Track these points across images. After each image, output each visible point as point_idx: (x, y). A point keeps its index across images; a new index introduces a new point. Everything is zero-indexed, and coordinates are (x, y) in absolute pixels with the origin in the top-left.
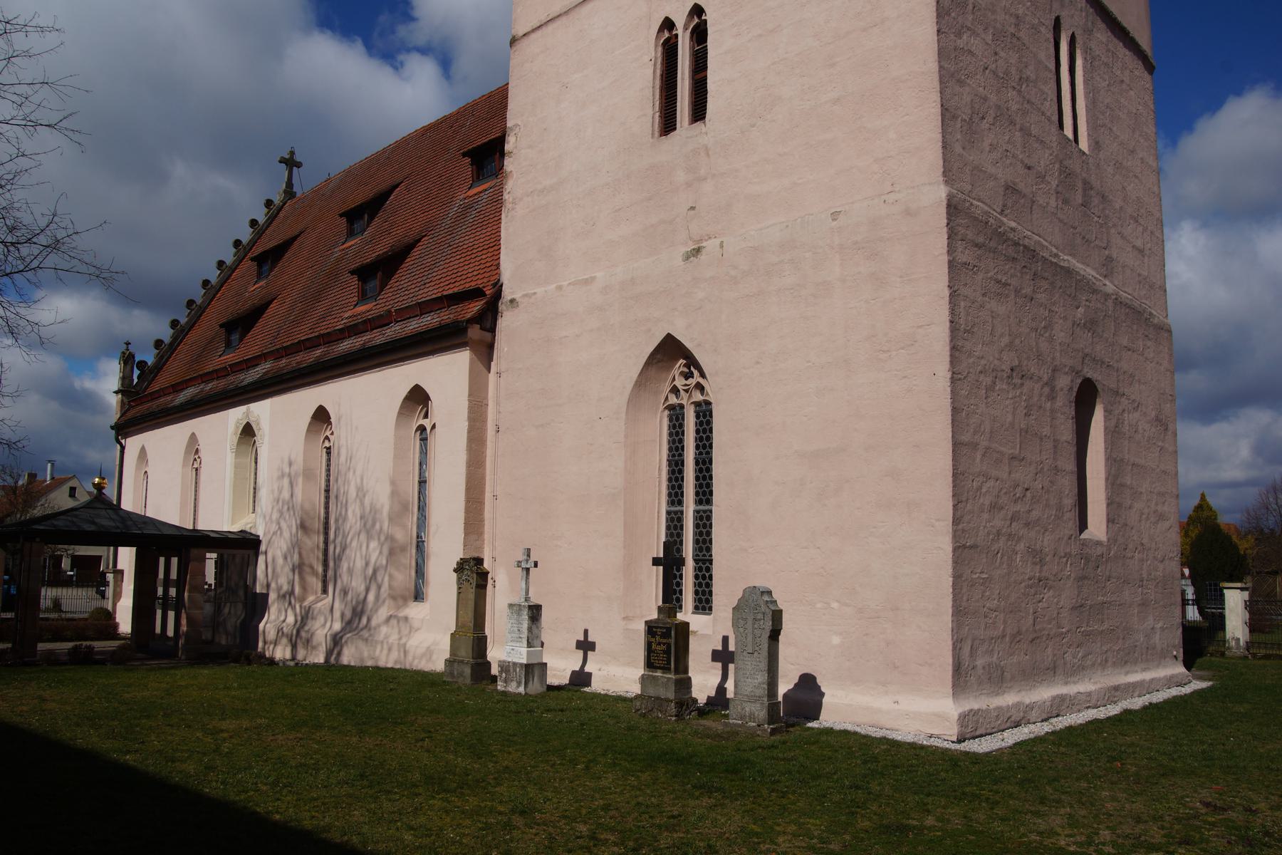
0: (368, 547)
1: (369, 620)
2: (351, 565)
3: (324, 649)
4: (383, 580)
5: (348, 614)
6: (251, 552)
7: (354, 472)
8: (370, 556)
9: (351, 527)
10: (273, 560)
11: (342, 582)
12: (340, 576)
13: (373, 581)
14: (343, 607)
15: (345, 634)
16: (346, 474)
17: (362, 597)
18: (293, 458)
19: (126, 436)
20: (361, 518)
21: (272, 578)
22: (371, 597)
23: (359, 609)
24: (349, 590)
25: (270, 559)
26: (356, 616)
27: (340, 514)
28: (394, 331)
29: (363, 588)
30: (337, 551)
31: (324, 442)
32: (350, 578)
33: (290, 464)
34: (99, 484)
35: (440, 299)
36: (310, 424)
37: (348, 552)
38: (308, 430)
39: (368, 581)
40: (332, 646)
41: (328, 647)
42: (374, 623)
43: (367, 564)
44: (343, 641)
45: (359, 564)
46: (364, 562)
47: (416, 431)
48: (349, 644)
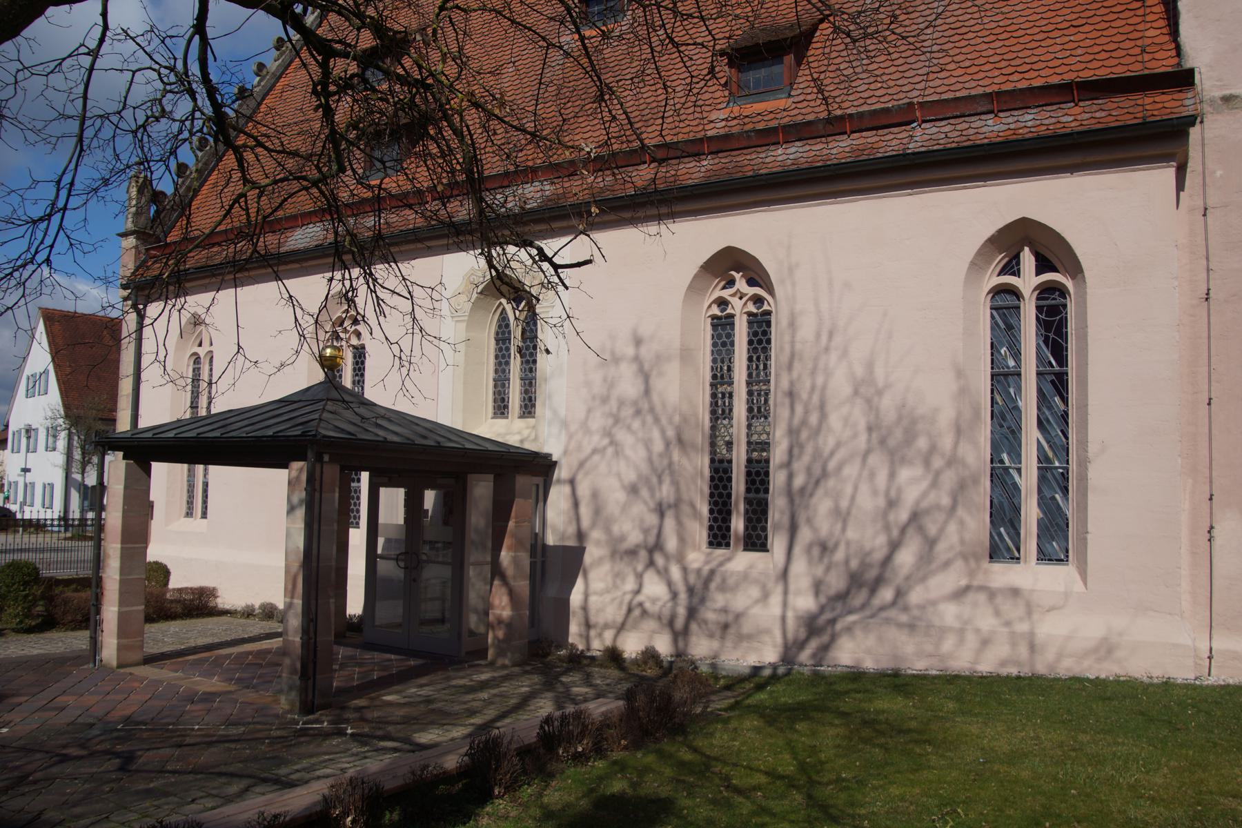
0: (892, 475)
1: (899, 594)
2: (844, 504)
3: (779, 639)
4: (942, 530)
5: (836, 582)
6: (539, 480)
7: (845, 353)
8: (899, 491)
9: (838, 445)
10: (595, 495)
11: (815, 530)
12: (809, 521)
13: (911, 531)
14: (819, 571)
15: (841, 616)
16: (816, 359)
17: (879, 556)
18: (645, 330)
19: (149, 300)
20: (870, 429)
21: (594, 525)
22: (906, 558)
23: (872, 574)
24: (836, 545)
25: (583, 490)
26: (861, 586)
27: (804, 422)
28: (923, 137)
29: (878, 543)
30: (799, 481)
31: (710, 306)
32: (839, 526)
33: (638, 342)
34: (333, 358)
35: (1047, 89)
36: (696, 277)
37: (831, 483)
38: (691, 287)
39: (895, 533)
40: (802, 634)
41: (790, 636)
42: (916, 596)
43: (892, 504)
44: (839, 626)
45: (868, 502)
46: (881, 502)
47: (988, 294)
48: (858, 632)
